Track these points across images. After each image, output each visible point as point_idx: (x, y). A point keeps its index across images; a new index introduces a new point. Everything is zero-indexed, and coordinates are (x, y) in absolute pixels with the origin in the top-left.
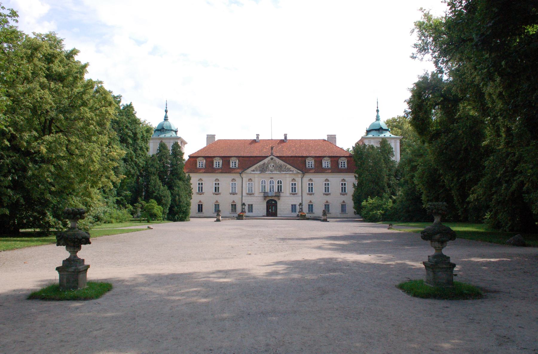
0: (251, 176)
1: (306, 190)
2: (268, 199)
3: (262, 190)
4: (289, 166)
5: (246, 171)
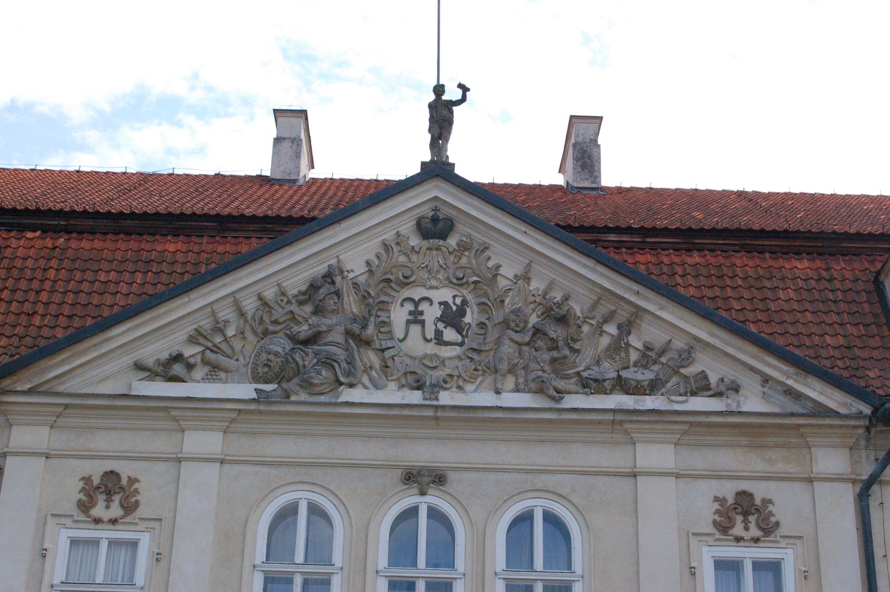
0: (113, 445)
4: (668, 322)
5: (53, 369)
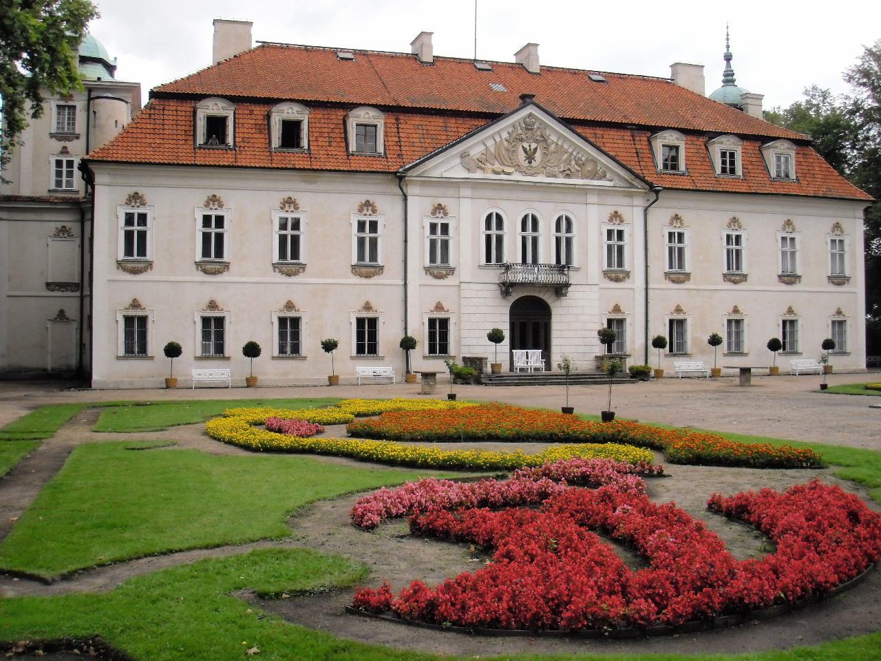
1: (660, 262)
2: (515, 296)
3: (488, 259)
